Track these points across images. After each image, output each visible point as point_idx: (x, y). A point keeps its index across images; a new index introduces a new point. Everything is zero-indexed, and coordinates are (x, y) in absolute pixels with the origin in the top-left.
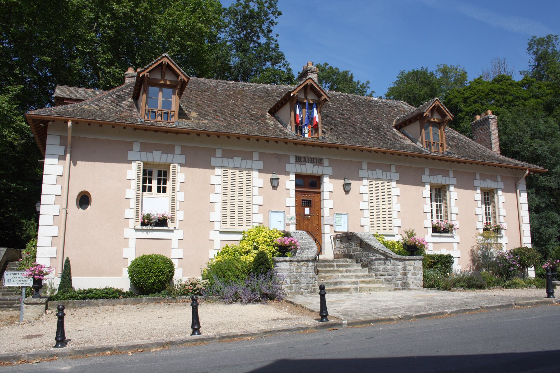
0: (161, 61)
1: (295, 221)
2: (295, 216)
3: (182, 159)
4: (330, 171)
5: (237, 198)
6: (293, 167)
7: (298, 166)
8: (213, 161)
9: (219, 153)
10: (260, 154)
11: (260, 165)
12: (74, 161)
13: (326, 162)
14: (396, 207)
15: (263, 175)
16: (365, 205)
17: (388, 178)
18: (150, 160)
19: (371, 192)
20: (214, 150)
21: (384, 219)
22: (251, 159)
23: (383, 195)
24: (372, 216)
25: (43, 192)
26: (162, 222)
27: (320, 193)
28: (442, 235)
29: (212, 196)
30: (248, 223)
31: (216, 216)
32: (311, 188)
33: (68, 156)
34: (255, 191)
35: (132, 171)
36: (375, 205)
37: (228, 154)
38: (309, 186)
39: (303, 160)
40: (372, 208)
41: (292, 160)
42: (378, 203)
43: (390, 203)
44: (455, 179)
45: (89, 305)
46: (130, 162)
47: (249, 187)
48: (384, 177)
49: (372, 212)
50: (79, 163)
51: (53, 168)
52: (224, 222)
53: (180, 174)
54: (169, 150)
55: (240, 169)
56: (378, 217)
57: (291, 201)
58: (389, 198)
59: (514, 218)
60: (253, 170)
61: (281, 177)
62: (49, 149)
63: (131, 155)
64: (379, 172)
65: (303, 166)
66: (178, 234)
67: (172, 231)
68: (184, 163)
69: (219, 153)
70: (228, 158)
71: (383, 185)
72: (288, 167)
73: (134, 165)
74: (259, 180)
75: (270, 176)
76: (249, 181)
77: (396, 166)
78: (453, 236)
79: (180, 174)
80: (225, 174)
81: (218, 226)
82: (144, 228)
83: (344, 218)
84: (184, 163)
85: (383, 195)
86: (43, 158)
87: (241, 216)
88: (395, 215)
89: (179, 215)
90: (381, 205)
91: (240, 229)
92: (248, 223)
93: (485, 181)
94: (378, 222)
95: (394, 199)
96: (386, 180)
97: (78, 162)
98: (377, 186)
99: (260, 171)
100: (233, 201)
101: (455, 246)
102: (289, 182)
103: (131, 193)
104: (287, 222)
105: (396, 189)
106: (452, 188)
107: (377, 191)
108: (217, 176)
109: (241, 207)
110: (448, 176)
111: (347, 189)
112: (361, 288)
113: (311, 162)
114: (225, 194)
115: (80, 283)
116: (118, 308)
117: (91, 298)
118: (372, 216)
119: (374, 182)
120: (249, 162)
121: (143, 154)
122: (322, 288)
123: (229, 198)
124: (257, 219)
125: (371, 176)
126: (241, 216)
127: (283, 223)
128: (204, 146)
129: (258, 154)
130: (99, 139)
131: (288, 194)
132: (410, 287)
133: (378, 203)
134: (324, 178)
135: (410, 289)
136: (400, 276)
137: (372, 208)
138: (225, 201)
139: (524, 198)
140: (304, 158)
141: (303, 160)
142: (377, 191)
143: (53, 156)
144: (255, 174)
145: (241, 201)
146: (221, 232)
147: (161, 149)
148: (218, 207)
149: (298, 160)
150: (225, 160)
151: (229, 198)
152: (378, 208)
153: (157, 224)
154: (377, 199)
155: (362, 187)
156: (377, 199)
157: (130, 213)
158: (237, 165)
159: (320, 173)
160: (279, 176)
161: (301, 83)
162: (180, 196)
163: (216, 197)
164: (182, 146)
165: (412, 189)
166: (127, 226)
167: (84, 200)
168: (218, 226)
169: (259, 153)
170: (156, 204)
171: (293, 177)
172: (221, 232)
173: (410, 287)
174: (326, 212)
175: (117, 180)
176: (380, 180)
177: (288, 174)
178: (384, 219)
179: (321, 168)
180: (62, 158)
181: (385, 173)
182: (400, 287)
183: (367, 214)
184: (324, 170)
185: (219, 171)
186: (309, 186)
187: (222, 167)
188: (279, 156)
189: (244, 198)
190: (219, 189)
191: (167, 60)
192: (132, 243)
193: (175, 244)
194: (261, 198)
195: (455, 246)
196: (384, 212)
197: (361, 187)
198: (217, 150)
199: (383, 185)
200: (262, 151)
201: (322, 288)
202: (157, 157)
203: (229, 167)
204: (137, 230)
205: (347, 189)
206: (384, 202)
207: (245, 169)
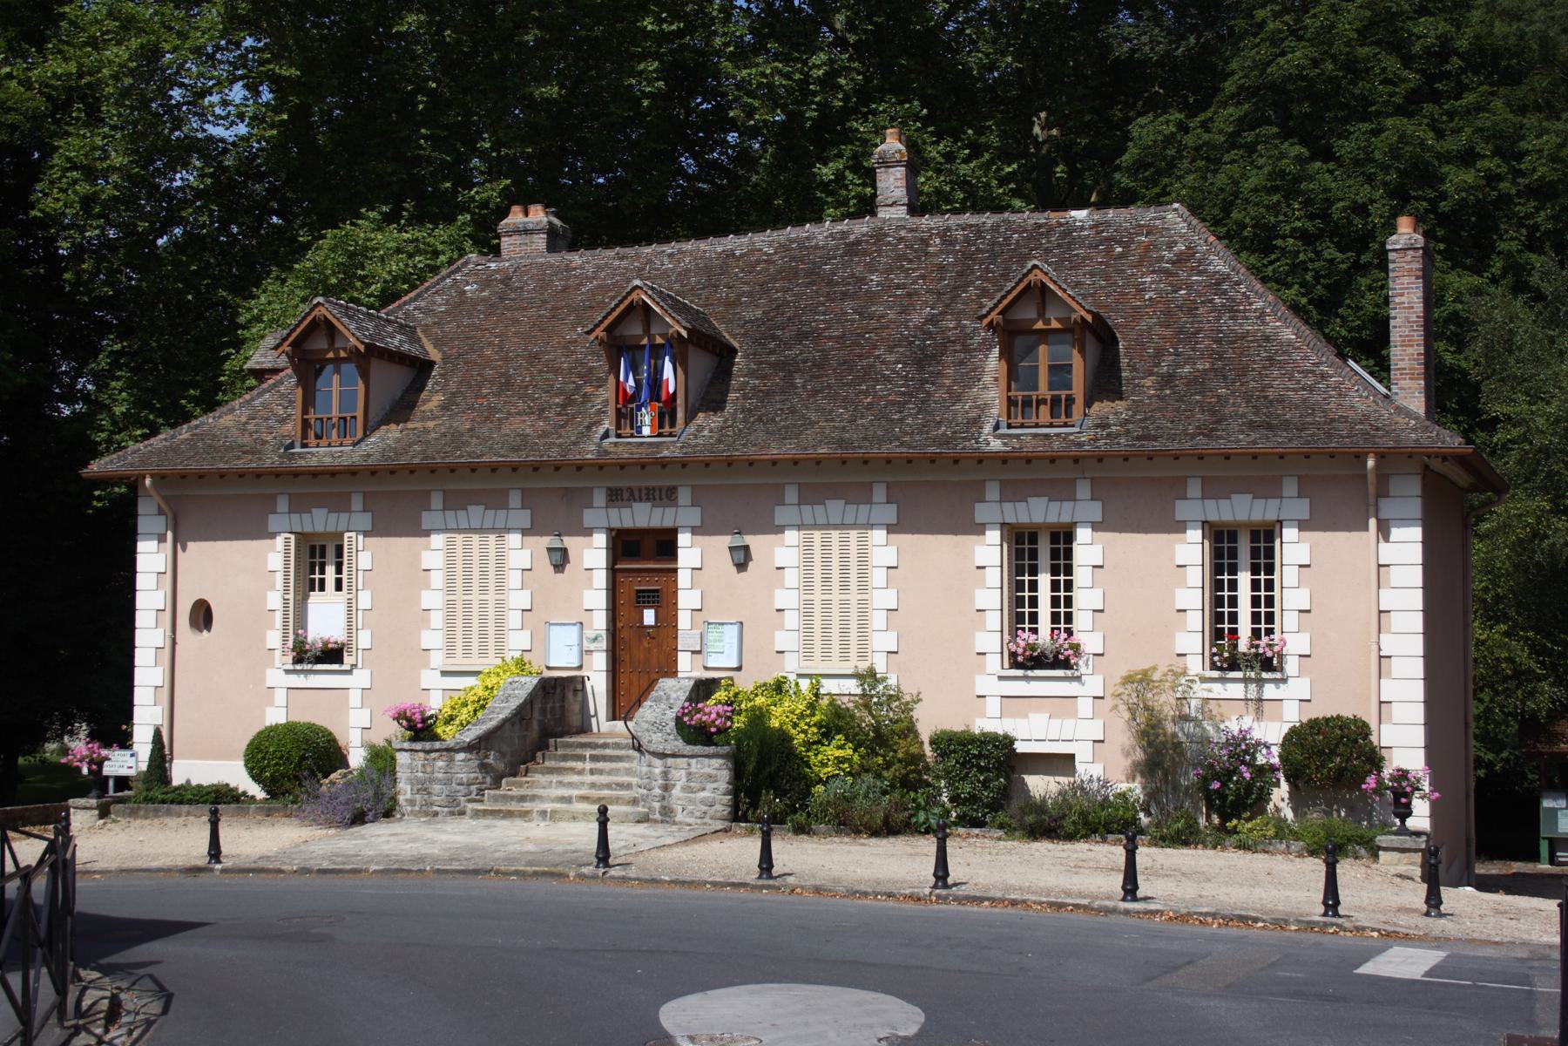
0: (1026, 282)
1: (603, 645)
2: (604, 633)
3: (365, 520)
5: (836, 596)
6: (603, 516)
7: (613, 512)
9: (437, 500)
10: (525, 492)
11: (524, 518)
12: (180, 541)
13: (684, 496)
14: (883, 598)
15: (531, 540)
16: (786, 598)
17: (862, 520)
18: (628, 523)
20: (428, 493)
21: (844, 631)
22: (869, 502)
23: (844, 569)
24: (808, 627)
25: (138, 606)
26: (332, 655)
27: (675, 570)
28: (1030, 673)
29: (425, 594)
30: (500, 650)
31: (432, 638)
32: (658, 561)
33: (170, 535)
34: (514, 579)
36: (459, 597)
37: (455, 502)
38: (642, 561)
39: (626, 495)
40: (809, 603)
41: (600, 498)
42: (827, 589)
44: (1098, 504)
45: (169, 813)
46: (273, 536)
48: (849, 520)
49: (808, 615)
50: (192, 546)
51: (150, 557)
52: (450, 651)
53: (364, 553)
54: (340, 504)
55: (481, 530)
56: (826, 629)
57: (596, 598)
58: (863, 575)
60: (508, 530)
61: (570, 542)
62: (143, 524)
63: (274, 522)
64: (835, 508)
65: (626, 512)
66: (361, 678)
67: (349, 672)
68: (369, 528)
69: (437, 500)
70: (812, 504)
71: (844, 543)
72: (982, 512)
73: (280, 541)
74: (520, 552)
75: (546, 541)
76: (501, 557)
78: (1078, 679)
79: (364, 553)
80: (450, 544)
81: (438, 660)
82: (298, 667)
83: (731, 632)
84: (369, 528)
85: (844, 569)
86: (135, 542)
87: (483, 636)
88: (878, 620)
89: (364, 639)
90: (836, 596)
91: (474, 663)
92: (500, 650)
93: (461, 513)
94: (826, 639)
95: (878, 577)
96: (854, 526)
97: (191, 545)
98: (826, 546)
99: (891, 529)
100: (467, 605)
101: (1085, 707)
102: (592, 553)
104: (586, 645)
105: (882, 547)
106: (1290, 533)
107: (826, 561)
108: (434, 551)
109: (483, 618)
111: (742, 559)
112: (554, 812)
113: (648, 499)
114: (451, 590)
115: (182, 772)
116: (171, 822)
117: (172, 802)
118: (808, 627)
119: (817, 535)
120: (502, 513)
121: (295, 517)
122: (603, 811)
123: (817, 597)
124: (518, 641)
125: (808, 520)
126: (483, 636)
127: (576, 649)
129: (1199, 481)
130: (221, 501)
131: (590, 579)
132: (677, 819)
133: (827, 589)
134: (680, 536)
135: (675, 823)
136: (657, 791)
137: (809, 603)
138: (450, 604)
139: (1406, 546)
140: (631, 490)
141: (626, 495)
142: (826, 561)
143: (149, 536)
145: (484, 603)
146: (445, 673)
147: (324, 506)
148: (437, 619)
149: (616, 497)
150: (806, 509)
152: (826, 604)
153: (319, 660)
154: (826, 579)
155: (783, 551)
156: (826, 579)
157: (274, 639)
158: (476, 524)
159: (668, 523)
160: (749, 540)
161: (1010, 285)
162: (365, 600)
163: (432, 599)
165: (938, 548)
166: (426, 665)
167: (203, 616)
168: (438, 660)
169: (523, 490)
170: (326, 618)
171: (600, 539)
172: (445, 673)
173: (677, 819)
174: (684, 620)
175: (248, 571)
176: (835, 527)
177: (588, 532)
178: (844, 631)
179: (670, 512)
180: (162, 539)
181: (851, 508)
182: (658, 816)
183: (792, 619)
184: (682, 514)
185: (791, 536)
186: (642, 561)
187: (446, 530)
188: (568, 493)
189: (854, 596)
190: (437, 579)
191: (1041, 276)
192: (280, 697)
193: (355, 698)
194: (892, 593)
195: (1085, 707)
196: (845, 612)
198: (433, 494)
199: (844, 543)
200: (529, 485)
201: (603, 811)
202: (319, 521)
203: (458, 530)
204: (287, 672)
205: (742, 559)
206: (845, 587)
207: (493, 530)
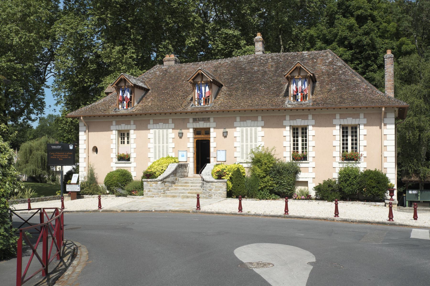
4: (214, 125)
7: (194, 124)
8: (235, 124)
9: (151, 122)
13: (212, 120)
18: (198, 127)
19: (242, 136)
23: (251, 138)
33: (87, 131)
34: (170, 140)
35: (114, 135)
36: (157, 145)
37: (156, 122)
39: (197, 120)
41: (191, 120)
43: (167, 143)
47: (167, 138)
51: (82, 136)
54: (128, 123)
59: (379, 149)
62: (80, 128)
63: (112, 127)
64: (249, 122)
65: (197, 124)
69: (151, 122)
70: (243, 121)
71: (251, 130)
75: (178, 131)
77: (262, 117)
99: (263, 127)
101: (311, 170)
103: (113, 146)
106: (362, 127)
109: (163, 150)
110: (307, 119)
111: (225, 135)
128: (143, 120)
134: (211, 129)
137: (243, 145)
138: (155, 147)
139: (390, 130)
140: (199, 118)
141: (197, 120)
143: (82, 131)
144: (260, 129)
145: (163, 146)
147: (125, 123)
148: (152, 150)
149: (195, 120)
151: (157, 145)
154: (247, 139)
156: (247, 139)
159: (208, 126)
160: (227, 130)
164: (172, 119)
165: (274, 132)
167: (95, 150)
170: (124, 150)
171: (191, 130)
176: (249, 127)
177: (189, 129)
179: (208, 123)
180: (85, 132)
184: (211, 125)
190: (152, 141)
195: (311, 170)
197: (188, 134)
202: (123, 127)
205: (225, 135)
